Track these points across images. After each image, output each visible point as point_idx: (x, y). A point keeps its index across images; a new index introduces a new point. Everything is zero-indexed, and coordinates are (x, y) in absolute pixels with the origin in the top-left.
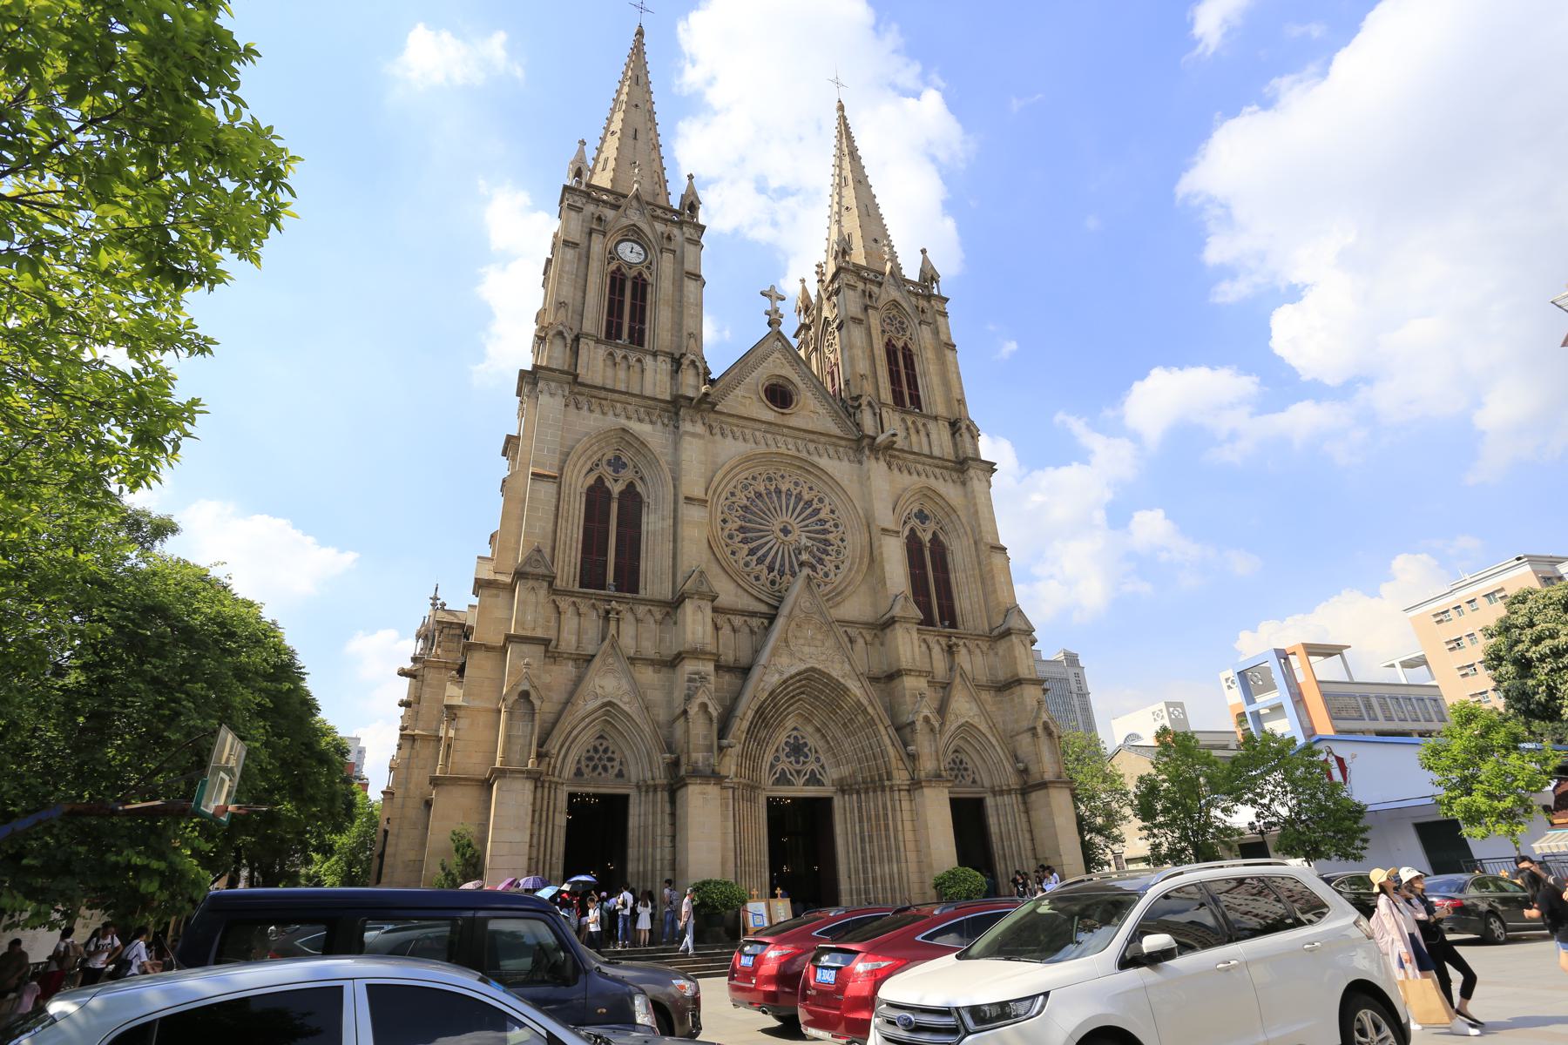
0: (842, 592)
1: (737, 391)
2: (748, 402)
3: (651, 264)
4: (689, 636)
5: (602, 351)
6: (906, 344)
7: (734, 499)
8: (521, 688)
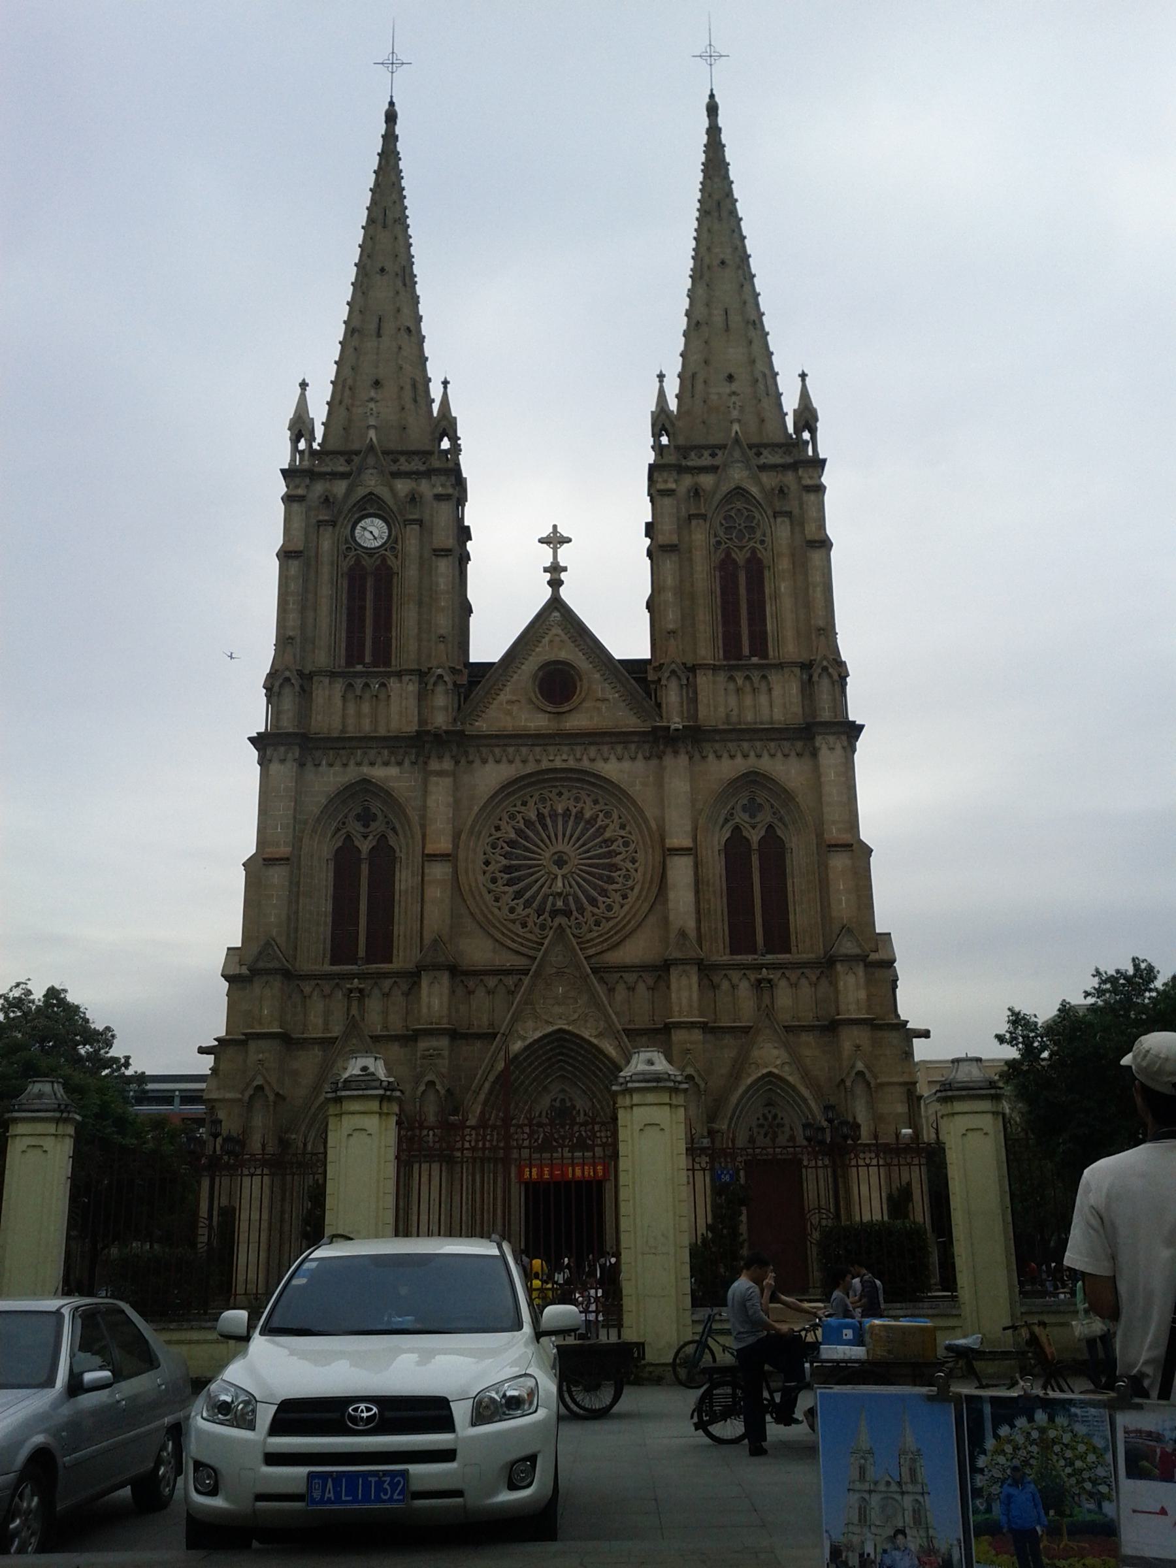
0: (624, 926)
1: (504, 697)
2: (515, 708)
3: (396, 542)
4: (424, 1010)
5: (339, 686)
6: (754, 551)
7: (498, 834)
8: (255, 1083)
